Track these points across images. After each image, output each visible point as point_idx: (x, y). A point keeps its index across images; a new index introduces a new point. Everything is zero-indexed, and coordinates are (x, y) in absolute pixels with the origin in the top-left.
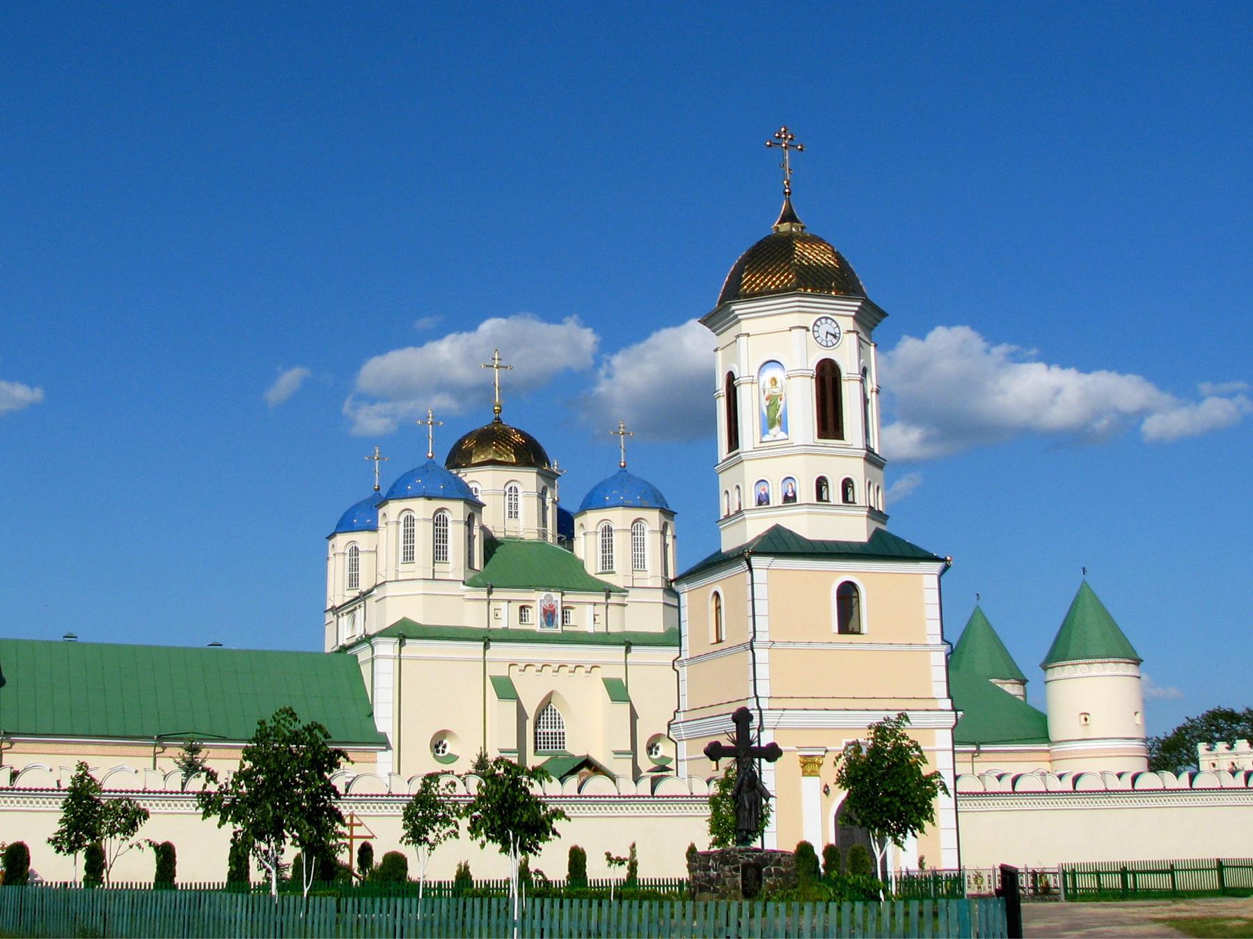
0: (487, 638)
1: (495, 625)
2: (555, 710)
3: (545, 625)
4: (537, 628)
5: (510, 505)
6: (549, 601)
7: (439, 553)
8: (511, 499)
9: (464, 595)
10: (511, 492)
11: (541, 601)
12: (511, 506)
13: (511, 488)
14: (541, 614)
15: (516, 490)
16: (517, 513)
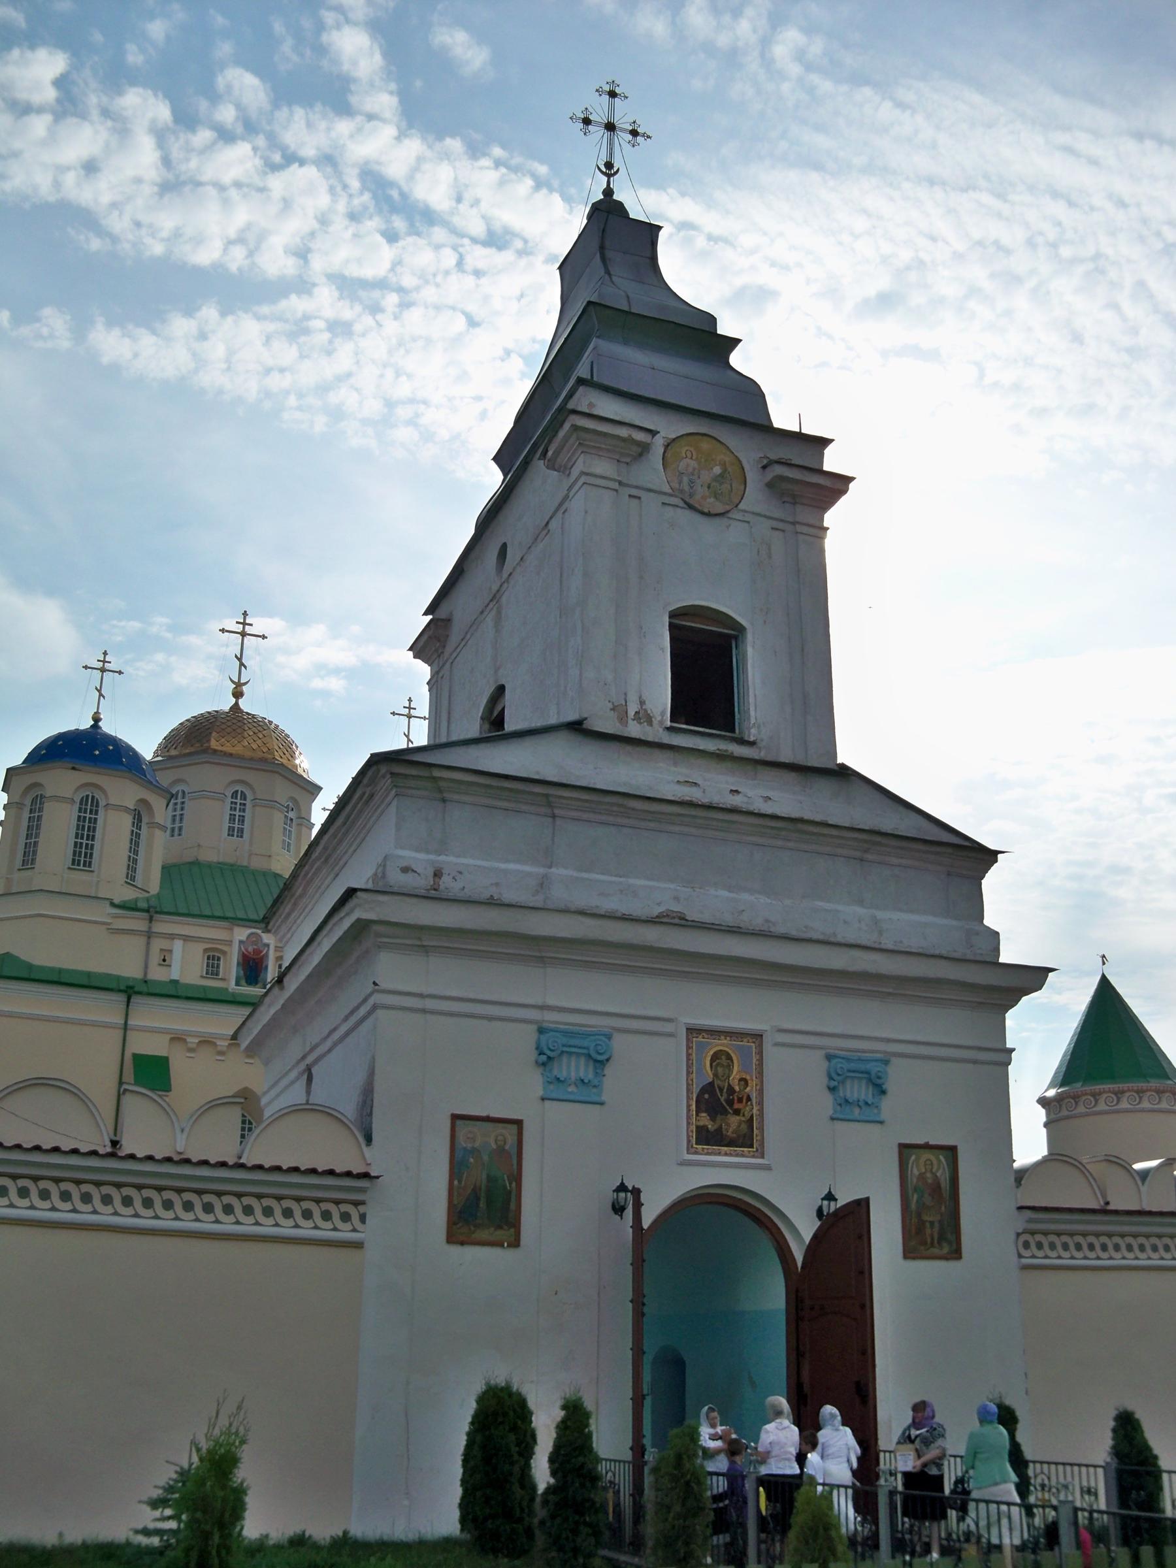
0: (129, 991)
1: (157, 974)
2: (250, 1123)
3: (243, 982)
4: (232, 985)
5: (232, 818)
6: (253, 943)
7: (83, 857)
8: (235, 809)
9: (109, 924)
10: (236, 798)
11: (241, 942)
12: (234, 820)
13: (237, 791)
14: (238, 964)
15: (244, 797)
16: (241, 831)
